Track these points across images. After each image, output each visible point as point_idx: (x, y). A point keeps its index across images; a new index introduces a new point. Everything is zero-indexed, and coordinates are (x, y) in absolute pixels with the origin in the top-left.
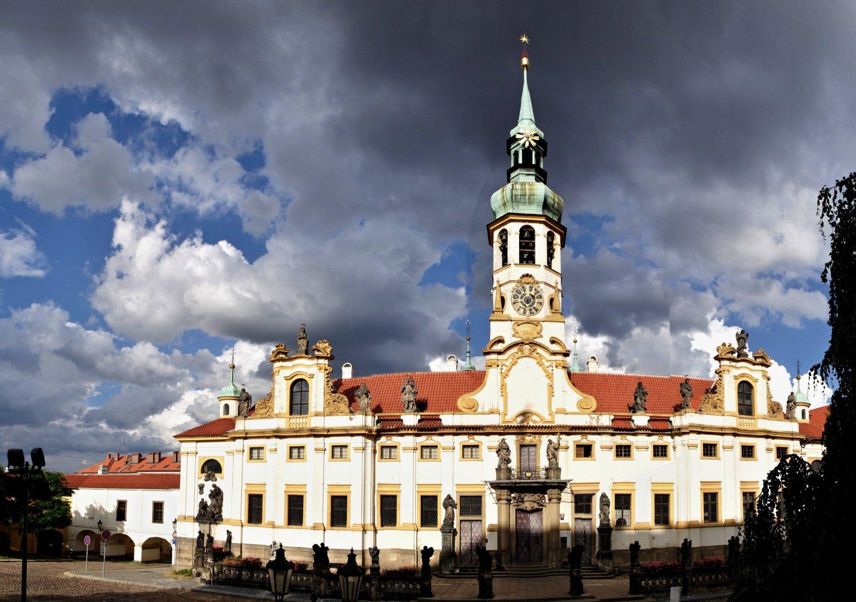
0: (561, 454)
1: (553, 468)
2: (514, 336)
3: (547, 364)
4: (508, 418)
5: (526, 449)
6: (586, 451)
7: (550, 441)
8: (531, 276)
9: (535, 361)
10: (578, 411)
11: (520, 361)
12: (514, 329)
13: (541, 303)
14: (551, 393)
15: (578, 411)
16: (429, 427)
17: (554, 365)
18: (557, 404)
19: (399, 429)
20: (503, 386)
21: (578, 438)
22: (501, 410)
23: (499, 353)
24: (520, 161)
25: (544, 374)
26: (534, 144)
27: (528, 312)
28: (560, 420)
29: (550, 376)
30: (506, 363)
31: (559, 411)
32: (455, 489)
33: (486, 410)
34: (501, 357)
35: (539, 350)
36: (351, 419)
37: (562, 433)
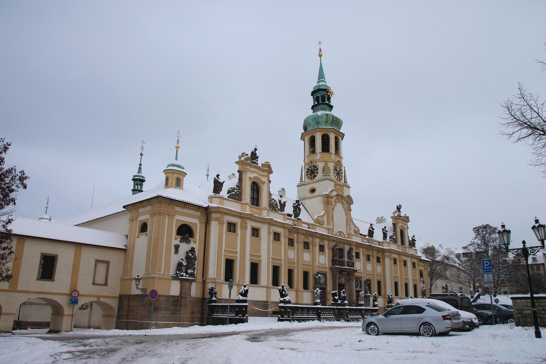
20: (333, 215)
23: (332, 197)
24: (320, 102)
29: (346, 214)
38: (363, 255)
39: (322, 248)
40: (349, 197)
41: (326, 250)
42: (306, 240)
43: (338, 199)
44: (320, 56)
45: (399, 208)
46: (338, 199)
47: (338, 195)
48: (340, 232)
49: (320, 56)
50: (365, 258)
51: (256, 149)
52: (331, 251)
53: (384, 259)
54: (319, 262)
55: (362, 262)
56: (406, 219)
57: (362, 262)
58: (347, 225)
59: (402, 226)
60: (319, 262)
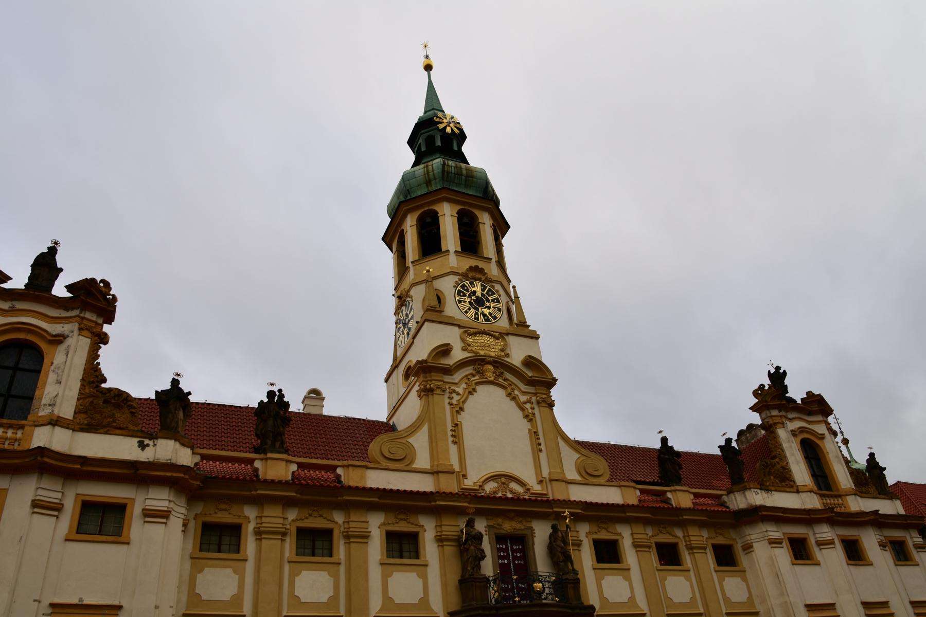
1: (567, 581)
2: (464, 349)
4: (469, 483)
6: (607, 553)
7: (554, 528)
8: (481, 271)
9: (500, 392)
10: (578, 478)
11: (479, 388)
12: (463, 340)
15: (578, 478)
17: (534, 399)
19: (251, 490)
22: (457, 468)
23: (448, 371)
25: (520, 414)
26: (457, 131)
28: (557, 493)
29: (529, 418)
30: (457, 389)
34: (447, 378)
36: (142, 446)
38: (636, 546)
39: (402, 546)
40: (533, 363)
41: (430, 549)
43: (481, 373)
44: (428, 68)
45: (778, 377)
46: (481, 373)
47: (477, 362)
49: (428, 68)
50: (653, 558)
51: (53, 251)
52: (450, 550)
53: (748, 548)
54: (387, 600)
55: (635, 573)
56: (816, 406)
57: (635, 573)
58: (537, 449)
59: (802, 430)
60: (387, 600)
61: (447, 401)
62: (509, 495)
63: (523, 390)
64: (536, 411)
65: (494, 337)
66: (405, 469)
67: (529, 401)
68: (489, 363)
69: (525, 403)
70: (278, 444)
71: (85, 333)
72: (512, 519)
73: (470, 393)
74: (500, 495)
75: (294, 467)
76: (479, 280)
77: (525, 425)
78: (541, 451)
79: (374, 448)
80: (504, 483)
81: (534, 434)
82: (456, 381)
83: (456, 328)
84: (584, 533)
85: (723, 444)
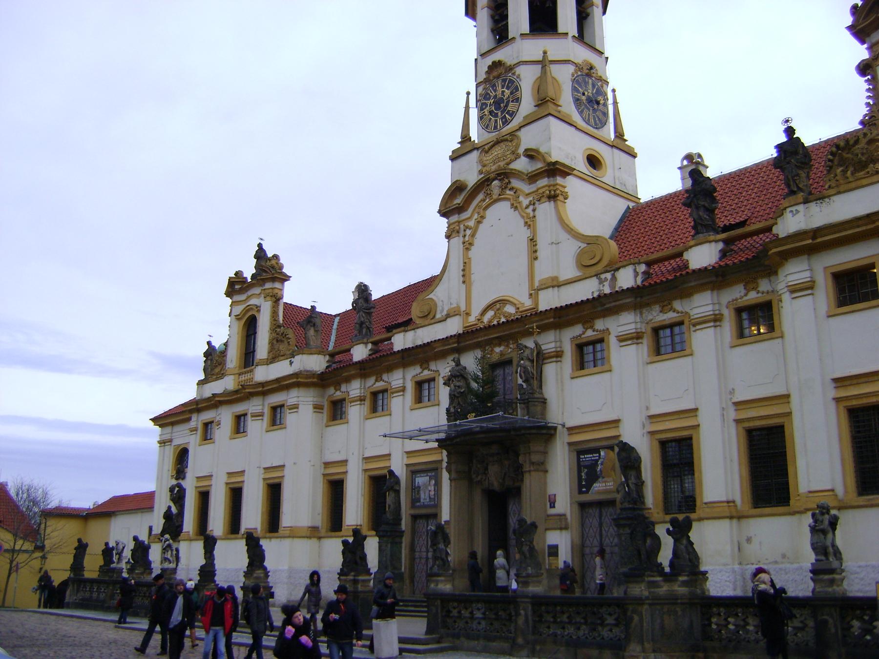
0: (550, 370)
1: (533, 398)
3: (525, 202)
4: (472, 319)
5: (499, 372)
11: (489, 212)
12: (481, 161)
13: (518, 100)
14: (533, 255)
16: (383, 361)
18: (543, 271)
21: (577, 330)
22: (463, 308)
25: (522, 222)
27: (500, 123)
29: (530, 223)
31: (544, 286)
32: (407, 461)
33: (445, 313)
35: (515, 183)
37: (544, 329)
39: (422, 391)
42: (380, 385)
43: (489, 195)
48: (497, 304)
61: (462, 239)
62: (503, 320)
63: (527, 192)
64: (537, 213)
65: (507, 140)
66: (433, 321)
67: (532, 203)
68: (494, 180)
69: (527, 207)
70: (364, 330)
71: (269, 298)
72: (500, 345)
73: (479, 222)
74: (495, 323)
75: (370, 346)
76: (498, 77)
77: (526, 233)
78: (536, 259)
79: (416, 311)
80: (498, 309)
81: (532, 241)
82: (469, 216)
83: (475, 152)
84: (565, 339)
85: (783, 139)
